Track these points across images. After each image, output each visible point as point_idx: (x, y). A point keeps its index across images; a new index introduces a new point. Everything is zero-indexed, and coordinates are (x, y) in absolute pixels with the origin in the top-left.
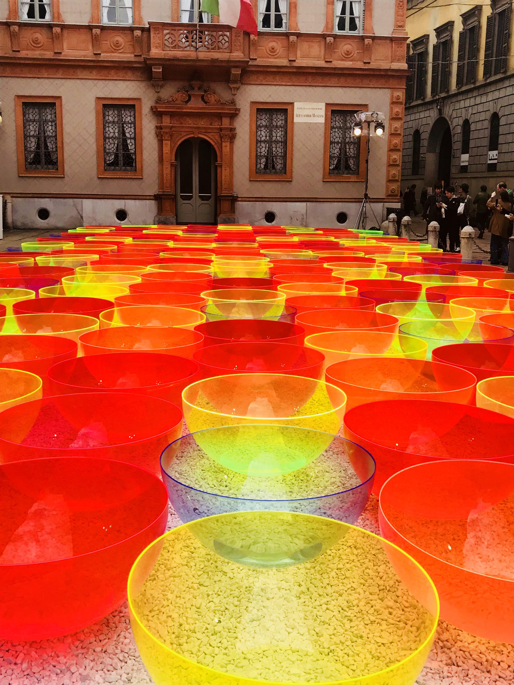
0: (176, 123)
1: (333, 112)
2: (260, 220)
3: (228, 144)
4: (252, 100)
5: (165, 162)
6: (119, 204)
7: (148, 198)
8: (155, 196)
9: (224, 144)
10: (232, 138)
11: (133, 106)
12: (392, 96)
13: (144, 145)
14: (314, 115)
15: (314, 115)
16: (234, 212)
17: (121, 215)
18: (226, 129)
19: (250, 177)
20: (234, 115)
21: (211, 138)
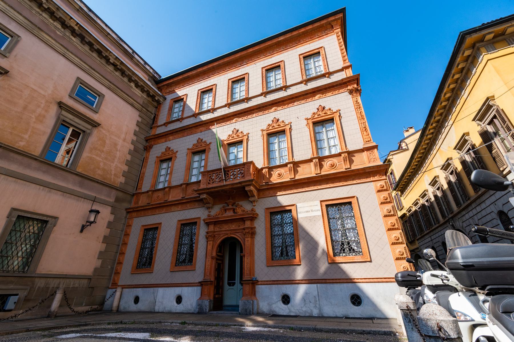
0: (217, 229)
1: (327, 206)
2: (277, 302)
3: (249, 239)
4: (266, 207)
5: (208, 257)
6: (177, 291)
7: (196, 284)
8: (200, 282)
9: (246, 239)
10: (253, 233)
11: (196, 223)
12: (376, 187)
13: (199, 246)
14: (312, 211)
15: (312, 211)
16: (255, 295)
17: (179, 300)
18: (248, 228)
19: (267, 263)
20: (253, 217)
21: (238, 236)
